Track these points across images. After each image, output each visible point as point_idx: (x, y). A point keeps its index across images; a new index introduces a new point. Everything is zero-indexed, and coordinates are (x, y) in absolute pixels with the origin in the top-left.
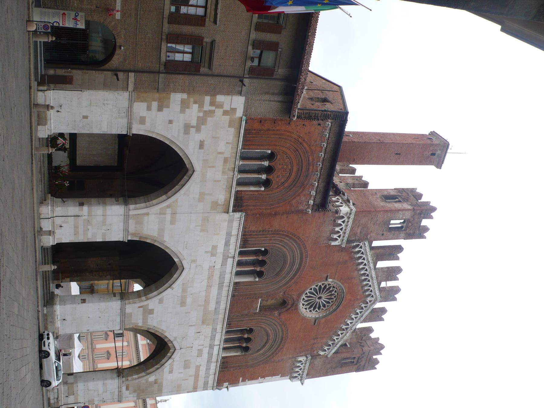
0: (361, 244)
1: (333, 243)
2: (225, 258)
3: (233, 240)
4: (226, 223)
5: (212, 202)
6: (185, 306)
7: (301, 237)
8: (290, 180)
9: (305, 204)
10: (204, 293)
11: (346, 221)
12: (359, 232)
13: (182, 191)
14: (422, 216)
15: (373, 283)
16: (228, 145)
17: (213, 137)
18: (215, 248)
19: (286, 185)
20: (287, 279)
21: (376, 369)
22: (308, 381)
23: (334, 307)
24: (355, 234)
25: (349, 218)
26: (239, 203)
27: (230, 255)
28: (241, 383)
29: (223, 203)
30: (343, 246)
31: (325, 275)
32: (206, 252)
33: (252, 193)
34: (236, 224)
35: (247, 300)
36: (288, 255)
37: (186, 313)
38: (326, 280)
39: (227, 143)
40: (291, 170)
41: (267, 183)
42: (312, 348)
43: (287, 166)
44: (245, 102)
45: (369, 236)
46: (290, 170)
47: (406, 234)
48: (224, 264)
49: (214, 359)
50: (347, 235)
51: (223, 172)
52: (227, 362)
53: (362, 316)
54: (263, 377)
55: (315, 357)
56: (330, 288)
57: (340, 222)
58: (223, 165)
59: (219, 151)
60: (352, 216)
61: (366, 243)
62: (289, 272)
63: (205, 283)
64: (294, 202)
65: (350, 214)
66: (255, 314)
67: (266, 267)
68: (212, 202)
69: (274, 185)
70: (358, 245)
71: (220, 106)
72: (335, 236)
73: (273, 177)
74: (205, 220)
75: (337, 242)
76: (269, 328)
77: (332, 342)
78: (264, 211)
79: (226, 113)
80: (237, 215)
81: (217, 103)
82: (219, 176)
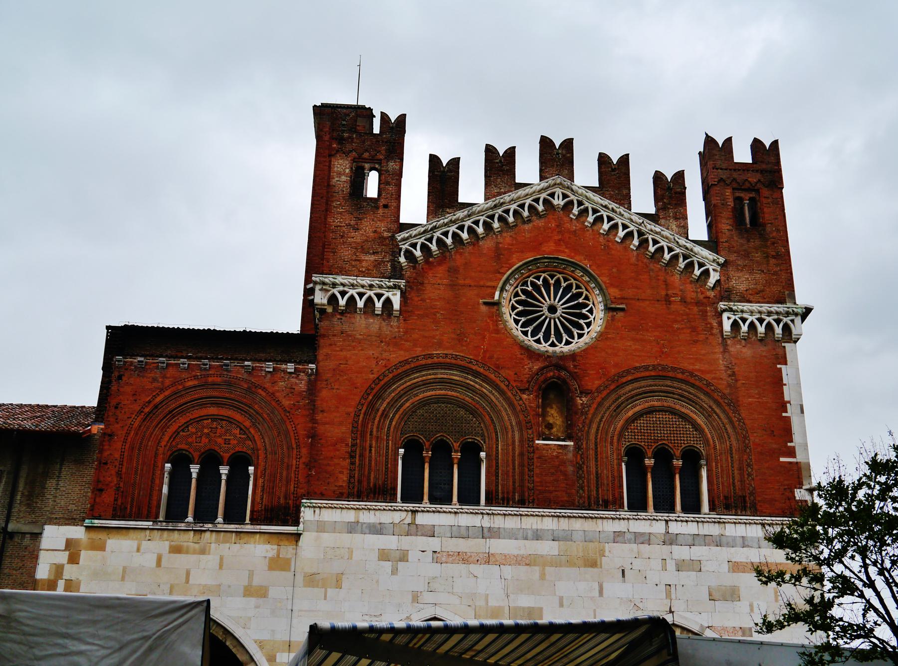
0: (405, 247)
1: (396, 305)
2: (413, 529)
3: (367, 517)
4: (325, 536)
5: (271, 568)
6: (541, 609)
7: (375, 376)
8: (238, 417)
9: (293, 380)
10: (508, 571)
11: (341, 288)
12: (372, 258)
13: (238, 633)
14: (346, 135)
15: (513, 201)
16: (142, 548)
17: (123, 579)
18: (384, 556)
19: (248, 423)
20: (486, 389)
21: (775, 143)
22: (802, 297)
23: (579, 273)
24: (377, 264)
25: (334, 285)
26: (282, 513)
27: (409, 520)
28: (800, 458)
29: (275, 547)
30: (402, 283)
31: (484, 308)
32: (394, 571)
33: (259, 491)
34: (329, 516)
35: (537, 471)
36: (421, 396)
37: (561, 605)
38: (498, 304)
39: (138, 550)
40: (215, 418)
41: (239, 463)
42: (698, 303)
43: (204, 427)
44: (55, 524)
45: (386, 234)
46: (213, 420)
47: (389, 158)
48: (431, 532)
49: (714, 530)
50: (376, 282)
51: (203, 552)
52: (726, 498)
53: (606, 207)
54: (783, 406)
55: (725, 292)
56: (524, 292)
57: (342, 302)
58: (187, 552)
59: (154, 565)
60: (329, 279)
61: (399, 238)
62: (468, 388)
63: (475, 569)
64: (286, 403)
65: (324, 283)
66: (578, 447)
67: (450, 440)
68: (271, 568)
69: (246, 448)
70: (409, 255)
71: (58, 570)
72: (379, 305)
73: (227, 451)
74: (312, 580)
75: (392, 298)
76: (629, 410)
77: (681, 259)
78: (303, 460)
79: (74, 559)
80: (306, 514)
81: (52, 578)
82: (210, 560)
